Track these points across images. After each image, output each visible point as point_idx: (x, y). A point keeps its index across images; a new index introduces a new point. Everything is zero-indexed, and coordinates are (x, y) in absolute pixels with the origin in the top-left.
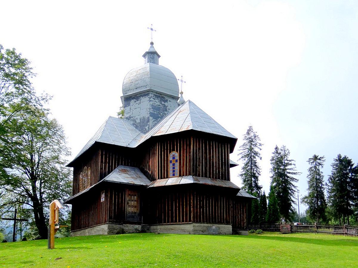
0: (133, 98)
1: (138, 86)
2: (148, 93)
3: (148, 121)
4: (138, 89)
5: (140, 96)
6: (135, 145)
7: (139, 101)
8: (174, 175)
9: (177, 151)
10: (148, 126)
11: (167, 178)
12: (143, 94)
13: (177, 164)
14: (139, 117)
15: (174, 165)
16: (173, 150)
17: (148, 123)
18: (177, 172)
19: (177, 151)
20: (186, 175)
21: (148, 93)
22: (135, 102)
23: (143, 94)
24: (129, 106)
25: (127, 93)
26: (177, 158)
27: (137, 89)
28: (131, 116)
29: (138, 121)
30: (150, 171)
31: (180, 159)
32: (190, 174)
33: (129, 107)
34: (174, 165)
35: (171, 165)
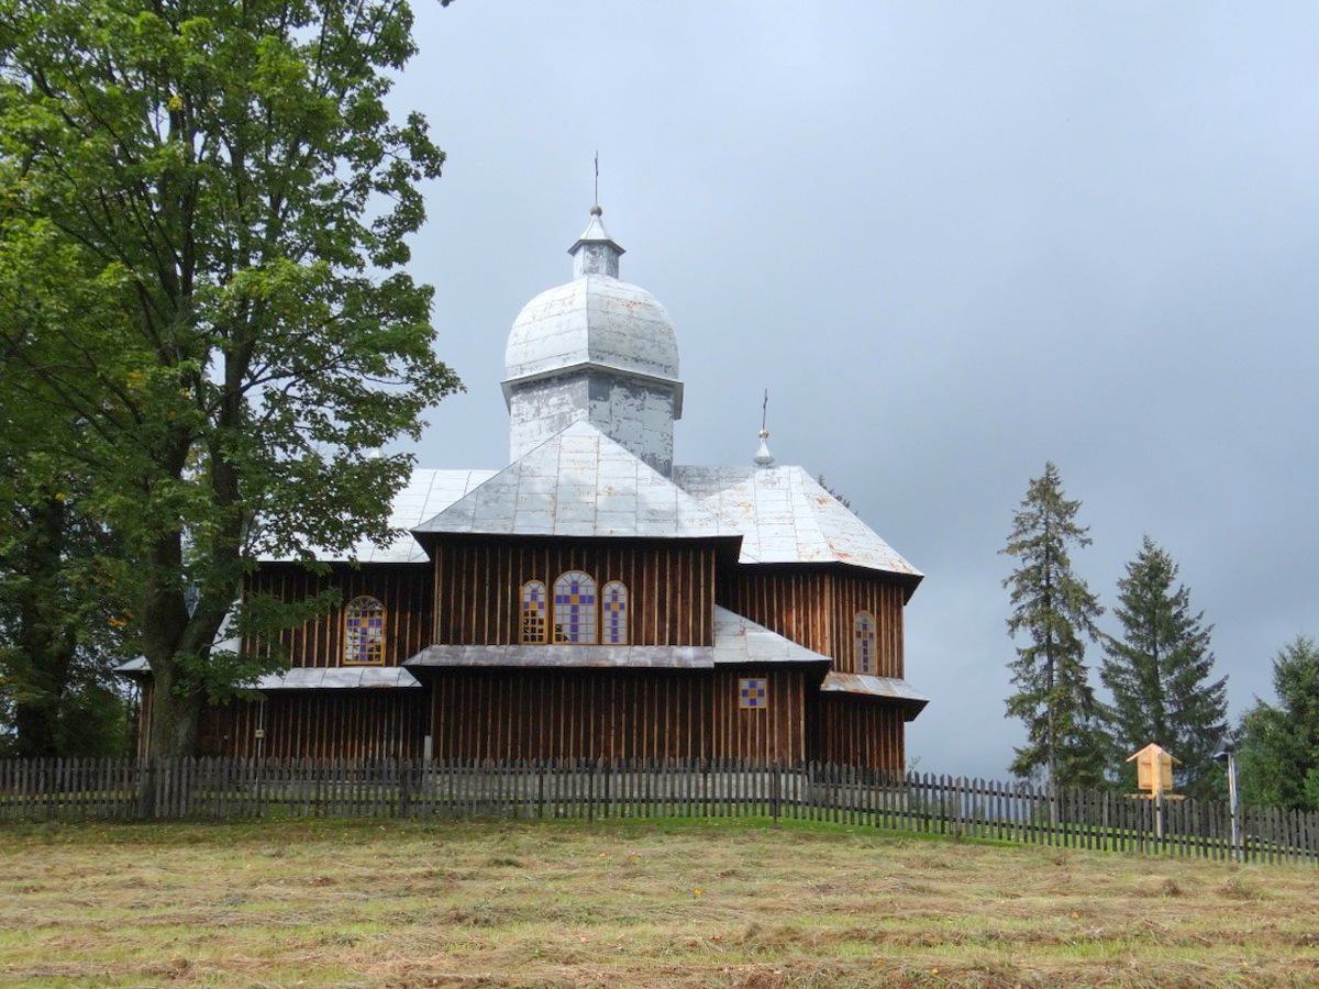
0: (621, 384)
1: (643, 355)
2: (667, 388)
4: (640, 363)
8: (866, 669)
11: (852, 671)
12: (652, 386)
13: (873, 645)
15: (865, 643)
18: (873, 662)
19: (872, 612)
20: (893, 676)
21: (667, 388)
22: (627, 397)
23: (652, 386)
24: (606, 400)
25: (602, 359)
27: (637, 361)
31: (879, 634)
34: (865, 643)
35: (857, 643)
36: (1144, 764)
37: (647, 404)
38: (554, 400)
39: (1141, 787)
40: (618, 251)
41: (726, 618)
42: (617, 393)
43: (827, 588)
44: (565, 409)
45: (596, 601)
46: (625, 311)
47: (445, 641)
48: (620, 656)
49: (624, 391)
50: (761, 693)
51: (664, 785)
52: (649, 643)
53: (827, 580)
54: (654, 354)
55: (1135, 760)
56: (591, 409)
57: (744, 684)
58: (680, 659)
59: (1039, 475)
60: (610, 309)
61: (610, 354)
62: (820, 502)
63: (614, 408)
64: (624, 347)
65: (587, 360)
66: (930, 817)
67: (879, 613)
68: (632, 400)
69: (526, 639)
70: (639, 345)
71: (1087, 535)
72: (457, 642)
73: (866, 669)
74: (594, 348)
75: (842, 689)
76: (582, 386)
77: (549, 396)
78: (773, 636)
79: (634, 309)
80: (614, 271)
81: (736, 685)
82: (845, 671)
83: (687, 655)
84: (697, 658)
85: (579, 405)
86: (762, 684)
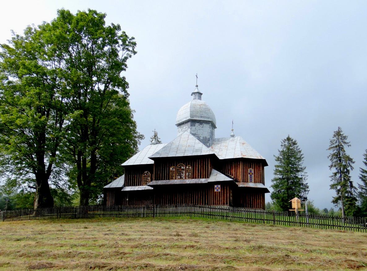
0: (198, 122)
1: (203, 116)
3: (209, 140)
5: (203, 123)
6: (221, 158)
7: (202, 126)
8: (251, 181)
9: (253, 168)
10: (209, 144)
11: (247, 182)
13: (253, 176)
14: (202, 136)
15: (251, 175)
16: (251, 167)
17: (209, 142)
18: (253, 180)
20: (258, 182)
23: (205, 122)
25: (193, 118)
26: (253, 172)
27: (201, 117)
28: (196, 134)
29: (201, 138)
30: (232, 175)
31: (255, 173)
32: (260, 182)
33: (195, 127)
34: (251, 175)
35: (249, 176)
36: (293, 202)
37: (204, 126)
38: (184, 127)
39: (293, 208)
40: (201, 94)
41: (215, 172)
42: (197, 124)
43: (241, 163)
44: (187, 129)
45: (185, 170)
46: (199, 107)
47: (155, 180)
48: (188, 181)
49: (199, 124)
50: (219, 188)
51: (180, 209)
52: (196, 178)
53: (241, 162)
54: (205, 115)
55: (291, 202)
56: (191, 129)
57: (216, 186)
58: (201, 181)
59: (337, 130)
60: (195, 107)
61: (195, 116)
62: (243, 144)
63: (196, 127)
64: (198, 115)
65: (190, 118)
66: (224, 216)
67: (255, 168)
68: (201, 126)
69: (171, 179)
70: (202, 114)
71: (349, 144)
72: (158, 180)
73: (251, 181)
74: (191, 116)
75: (243, 186)
76: (189, 124)
77: (184, 127)
78: (223, 175)
79: (201, 106)
80: (200, 98)
81: (214, 187)
82: (246, 182)
83: (203, 181)
84: (204, 181)
85: (189, 128)
86: (219, 186)
